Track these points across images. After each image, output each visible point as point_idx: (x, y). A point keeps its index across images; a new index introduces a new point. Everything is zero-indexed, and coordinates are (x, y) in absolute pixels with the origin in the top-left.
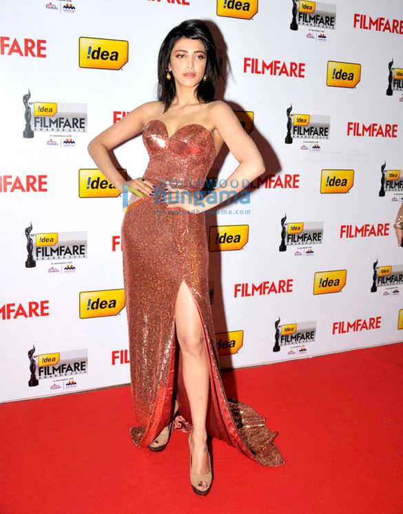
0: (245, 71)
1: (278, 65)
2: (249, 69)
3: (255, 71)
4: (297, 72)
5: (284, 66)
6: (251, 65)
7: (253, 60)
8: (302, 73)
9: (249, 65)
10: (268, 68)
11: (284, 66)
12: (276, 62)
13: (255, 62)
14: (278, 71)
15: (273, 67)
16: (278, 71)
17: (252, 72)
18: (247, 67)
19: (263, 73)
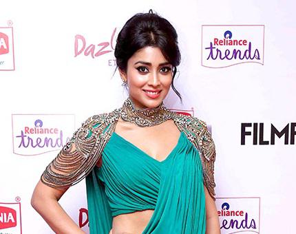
0: (243, 143)
2: (249, 139)
3: (259, 140)
6: (253, 133)
7: (256, 125)
9: (249, 133)
13: (258, 128)
17: (255, 143)
18: (247, 137)
19: (273, 143)
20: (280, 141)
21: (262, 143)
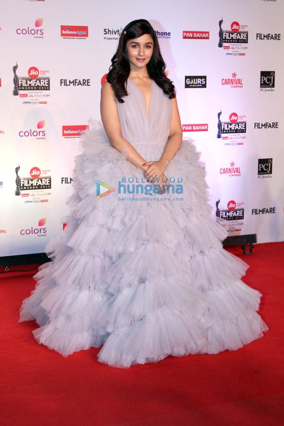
0: (61, 85)
1: (76, 81)
2: (63, 84)
4: (86, 83)
5: (80, 81)
8: (89, 84)
10: (72, 83)
11: (80, 81)
12: (76, 80)
13: (65, 81)
14: (77, 84)
15: (74, 82)
16: (77, 84)
20: (72, 85)
21: (67, 85)
